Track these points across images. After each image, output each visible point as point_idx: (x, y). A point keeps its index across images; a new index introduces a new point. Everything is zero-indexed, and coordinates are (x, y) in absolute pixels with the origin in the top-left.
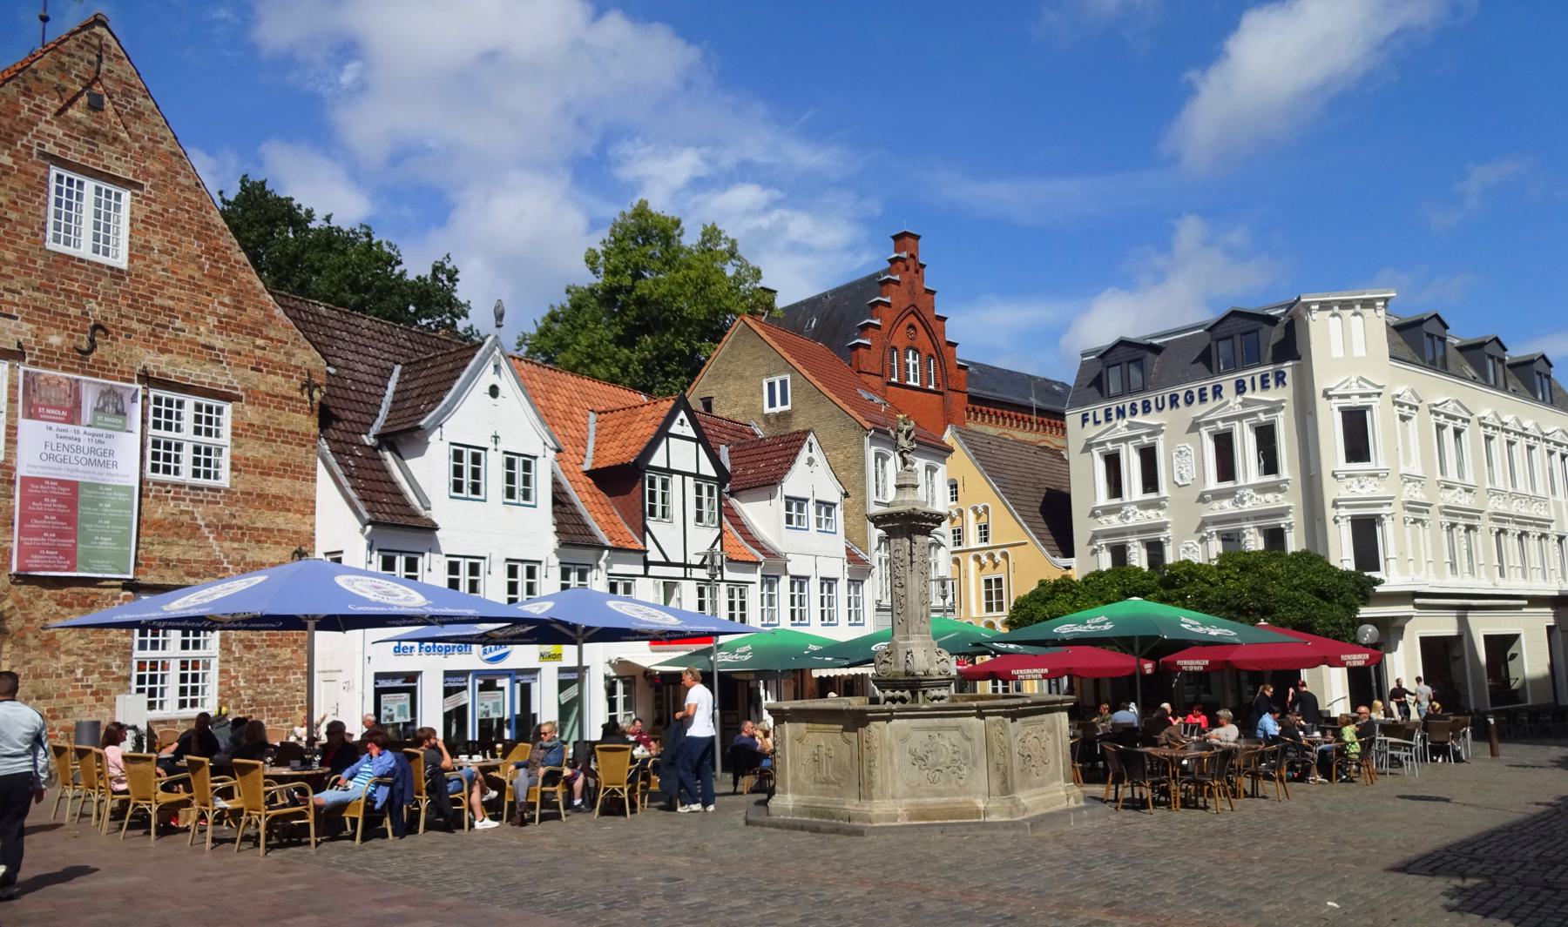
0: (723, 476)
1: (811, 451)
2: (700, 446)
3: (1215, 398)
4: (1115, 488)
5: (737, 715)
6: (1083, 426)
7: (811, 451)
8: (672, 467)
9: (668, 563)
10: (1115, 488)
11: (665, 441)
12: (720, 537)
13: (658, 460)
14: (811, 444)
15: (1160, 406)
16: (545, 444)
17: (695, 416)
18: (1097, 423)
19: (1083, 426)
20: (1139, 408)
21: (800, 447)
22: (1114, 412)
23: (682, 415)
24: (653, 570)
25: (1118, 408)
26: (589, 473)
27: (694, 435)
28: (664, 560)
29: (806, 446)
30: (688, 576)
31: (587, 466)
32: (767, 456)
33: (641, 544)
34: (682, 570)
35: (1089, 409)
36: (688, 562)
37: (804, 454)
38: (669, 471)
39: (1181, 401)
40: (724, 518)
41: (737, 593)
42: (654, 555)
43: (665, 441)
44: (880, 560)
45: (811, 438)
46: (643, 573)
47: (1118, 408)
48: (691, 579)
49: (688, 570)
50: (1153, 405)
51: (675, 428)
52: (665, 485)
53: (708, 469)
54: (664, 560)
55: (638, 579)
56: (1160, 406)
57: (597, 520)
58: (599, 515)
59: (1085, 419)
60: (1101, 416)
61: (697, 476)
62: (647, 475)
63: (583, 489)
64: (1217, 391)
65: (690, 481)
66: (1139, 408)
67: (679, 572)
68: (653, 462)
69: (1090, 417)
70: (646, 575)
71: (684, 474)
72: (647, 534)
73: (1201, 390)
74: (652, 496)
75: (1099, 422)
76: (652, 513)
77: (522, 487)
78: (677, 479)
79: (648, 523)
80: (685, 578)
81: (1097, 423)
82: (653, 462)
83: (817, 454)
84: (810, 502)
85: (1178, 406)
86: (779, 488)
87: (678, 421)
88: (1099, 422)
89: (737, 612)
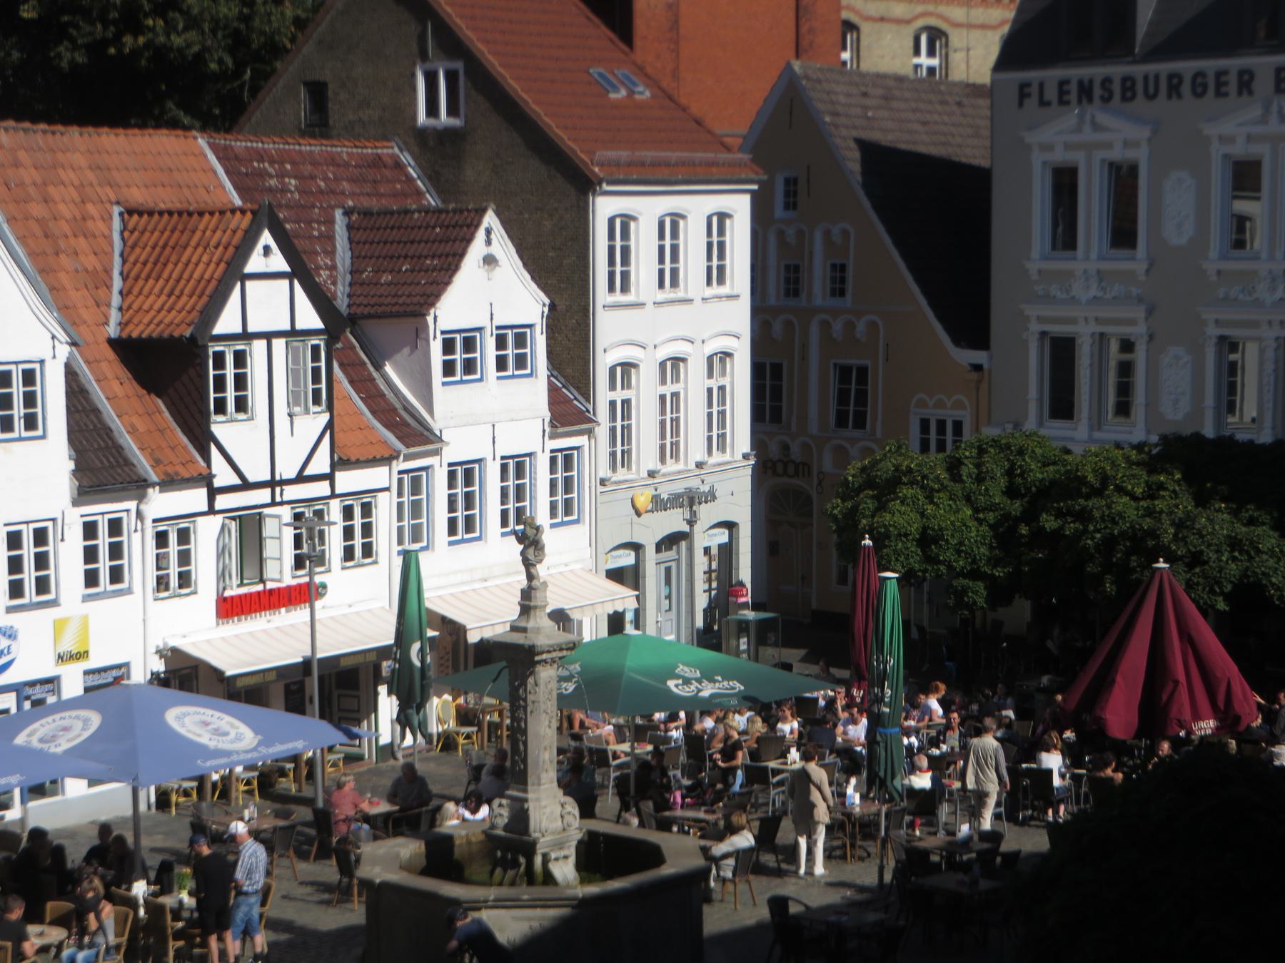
0: (335, 323)
1: (488, 242)
2: (296, 283)
4: (1065, 236)
5: (358, 697)
6: (1021, 104)
7: (488, 242)
8: (252, 328)
9: (246, 485)
10: (1065, 236)
11: (239, 285)
12: (330, 426)
13: (227, 322)
14: (488, 232)
15: (1151, 90)
16: (53, 337)
17: (284, 230)
19: (1021, 104)
21: (468, 240)
22: (1074, 88)
23: (266, 238)
24: (222, 502)
26: (114, 343)
27: (284, 267)
28: (237, 481)
29: (480, 235)
30: (278, 499)
31: (112, 330)
32: (412, 250)
33: (202, 463)
34: (268, 491)
36: (278, 478)
37: (477, 249)
38: (246, 336)
39: (1186, 88)
40: (336, 365)
41: (357, 511)
42: (224, 475)
43: (239, 285)
44: (613, 404)
45: (490, 219)
46: (206, 509)
47: (1081, 83)
48: (282, 503)
49: (278, 490)
51: (255, 263)
52: (240, 359)
53: (309, 318)
54: (237, 481)
55: (200, 520)
56: (1151, 90)
57: (133, 431)
58: (135, 420)
60: (1051, 93)
61: (293, 334)
62: (211, 351)
63: (110, 375)
64: (1246, 82)
65: (279, 345)
66: (1117, 88)
67: (263, 496)
68: (219, 329)
69: (1034, 90)
70: (211, 511)
71: (269, 336)
72: (213, 448)
74: (220, 384)
75: (1048, 104)
76: (221, 407)
77: (23, 411)
78: (259, 346)
79: (215, 429)
80: (273, 503)
82: (220, 328)
83: (503, 248)
84: (488, 332)
85: (1179, 96)
86: (430, 319)
87: (259, 248)
89: (358, 542)
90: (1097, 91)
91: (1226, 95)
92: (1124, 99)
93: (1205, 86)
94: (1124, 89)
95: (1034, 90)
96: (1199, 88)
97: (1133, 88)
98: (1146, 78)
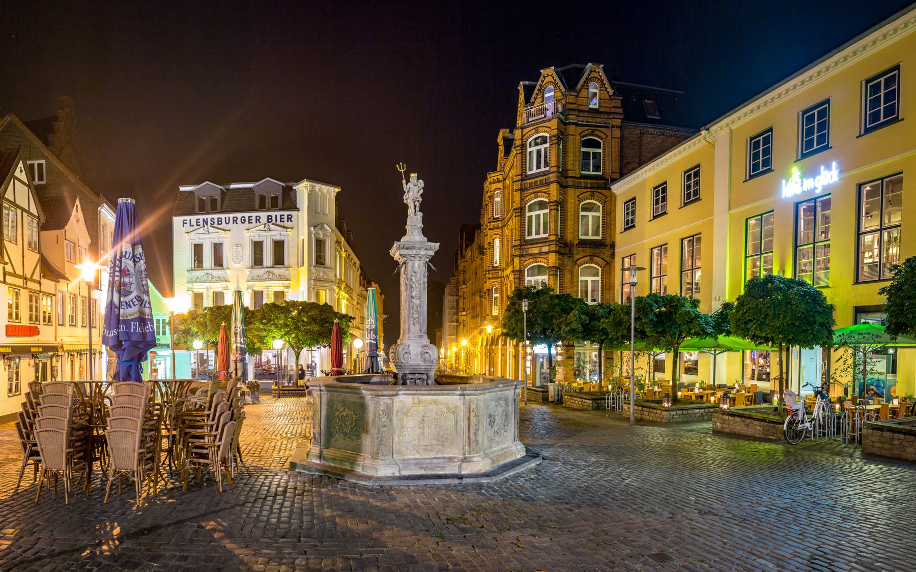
3: (256, 222)
15: (227, 222)
18: (191, 226)
20: (216, 221)
25: (204, 219)
35: (188, 218)
39: (239, 221)
47: (204, 219)
50: (223, 221)
56: (227, 222)
59: (184, 223)
60: (194, 223)
66: (216, 221)
69: (188, 222)
73: (249, 217)
75: (193, 226)
81: (191, 226)
85: (237, 223)
88: (193, 226)
90: (209, 222)
91: (252, 223)
92: (218, 224)
93: (245, 220)
94: (218, 221)
95: (188, 222)
96: (243, 222)
97: (221, 221)
98: (226, 218)
